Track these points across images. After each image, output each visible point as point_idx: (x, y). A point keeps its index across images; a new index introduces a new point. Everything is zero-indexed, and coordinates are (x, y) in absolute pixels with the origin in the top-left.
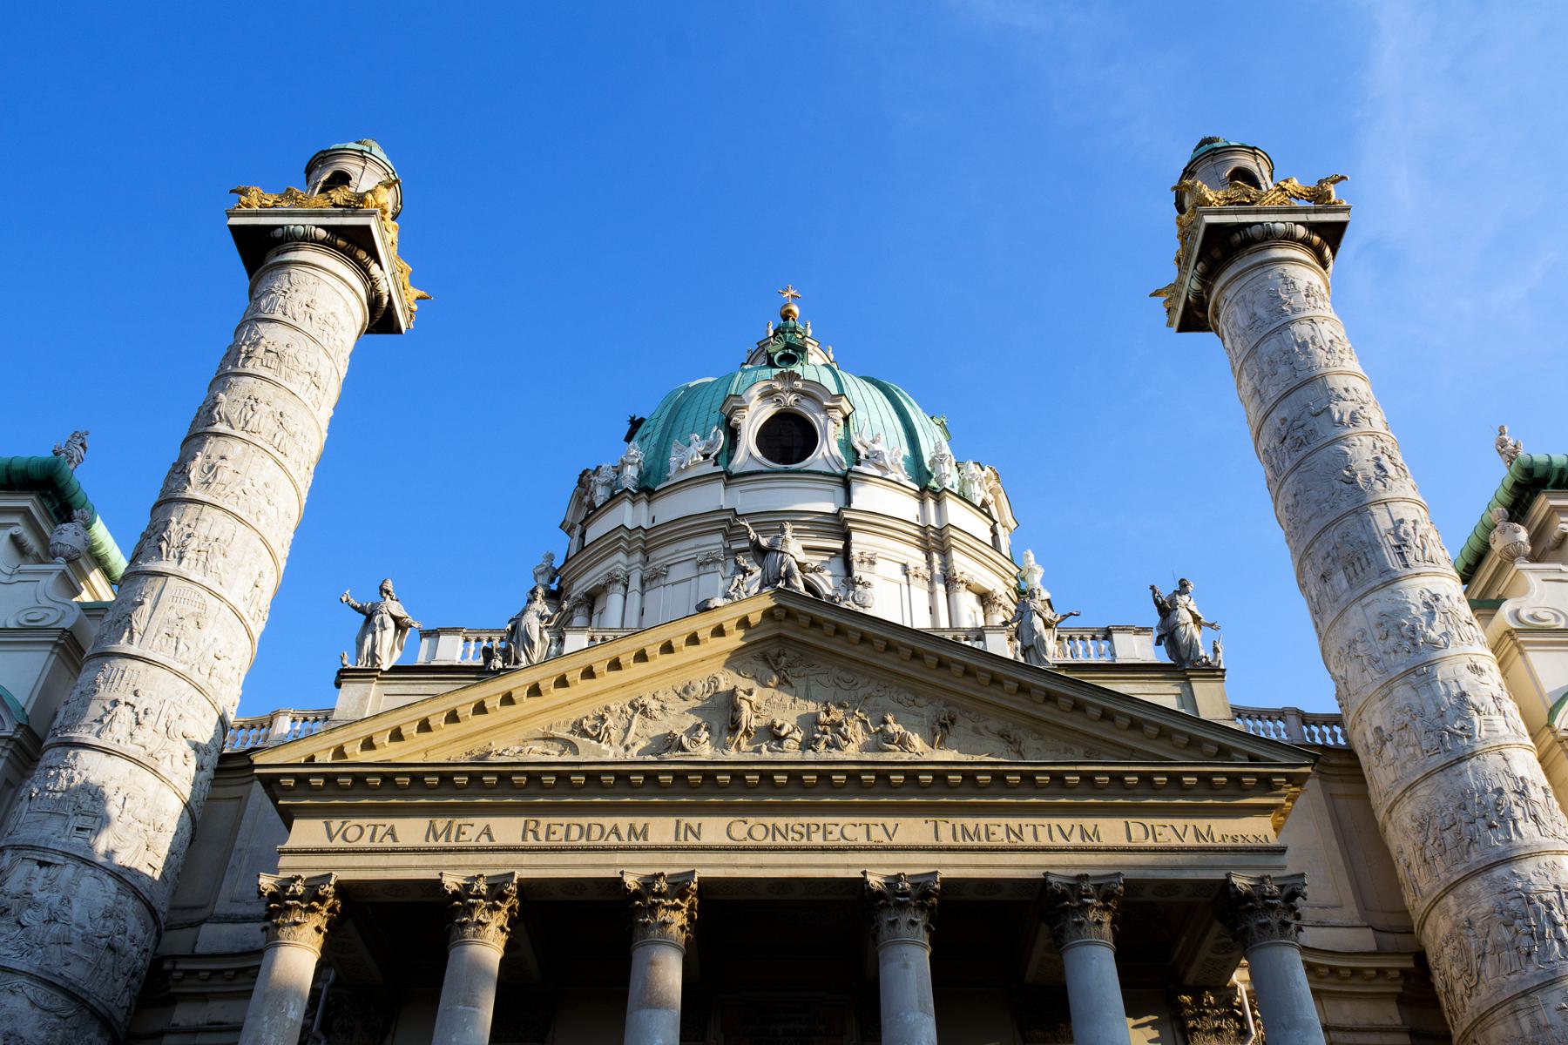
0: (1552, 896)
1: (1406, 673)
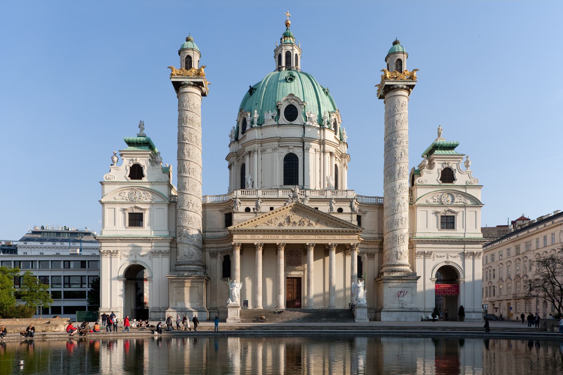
0: (399, 236)
1: (392, 198)
